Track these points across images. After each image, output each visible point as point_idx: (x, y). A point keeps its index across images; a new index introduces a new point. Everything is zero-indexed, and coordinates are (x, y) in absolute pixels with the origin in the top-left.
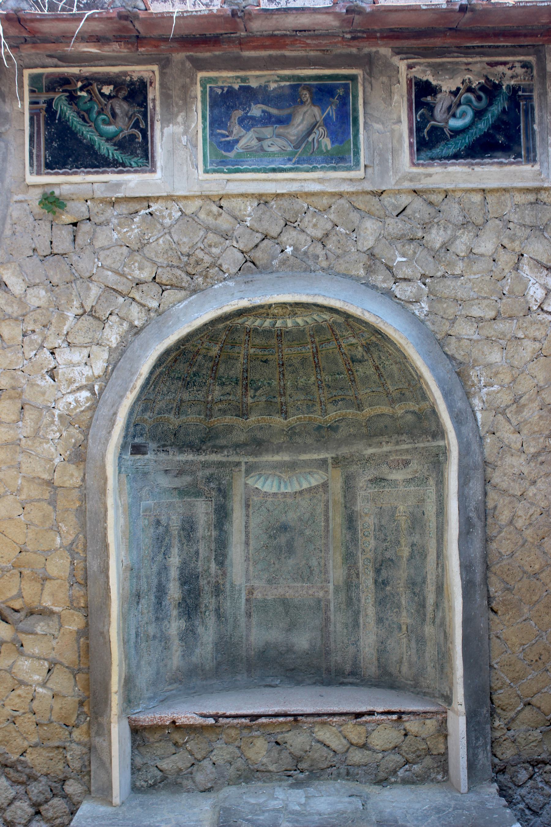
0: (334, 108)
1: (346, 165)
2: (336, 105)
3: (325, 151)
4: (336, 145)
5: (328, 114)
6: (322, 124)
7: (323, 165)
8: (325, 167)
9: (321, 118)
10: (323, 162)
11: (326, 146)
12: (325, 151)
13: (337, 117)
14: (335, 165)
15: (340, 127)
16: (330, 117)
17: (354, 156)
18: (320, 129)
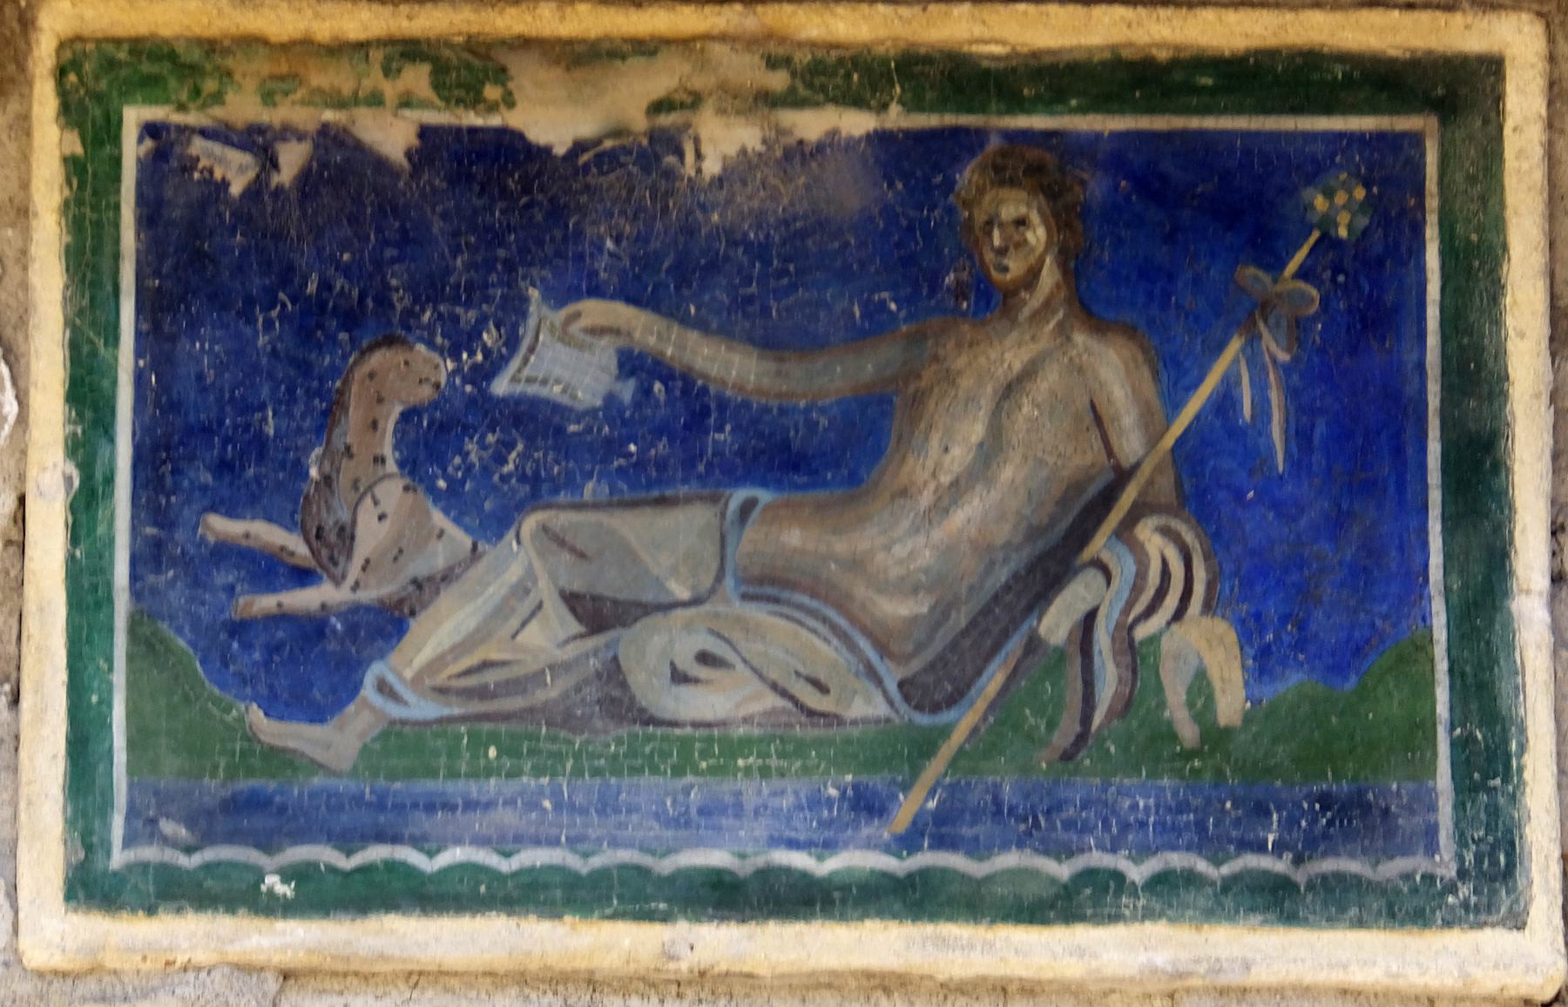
0: (1275, 349)
1: (1392, 868)
2: (1300, 326)
3: (1188, 732)
4: (1293, 682)
5: (1225, 402)
6: (1166, 483)
7: (1177, 860)
8: (1191, 879)
9: (1153, 441)
10: (1169, 837)
11: (1201, 686)
12: (1188, 732)
13: (1300, 436)
14: (1280, 865)
15: (1337, 523)
16: (1235, 432)
17: (1465, 788)
18: (1148, 533)
